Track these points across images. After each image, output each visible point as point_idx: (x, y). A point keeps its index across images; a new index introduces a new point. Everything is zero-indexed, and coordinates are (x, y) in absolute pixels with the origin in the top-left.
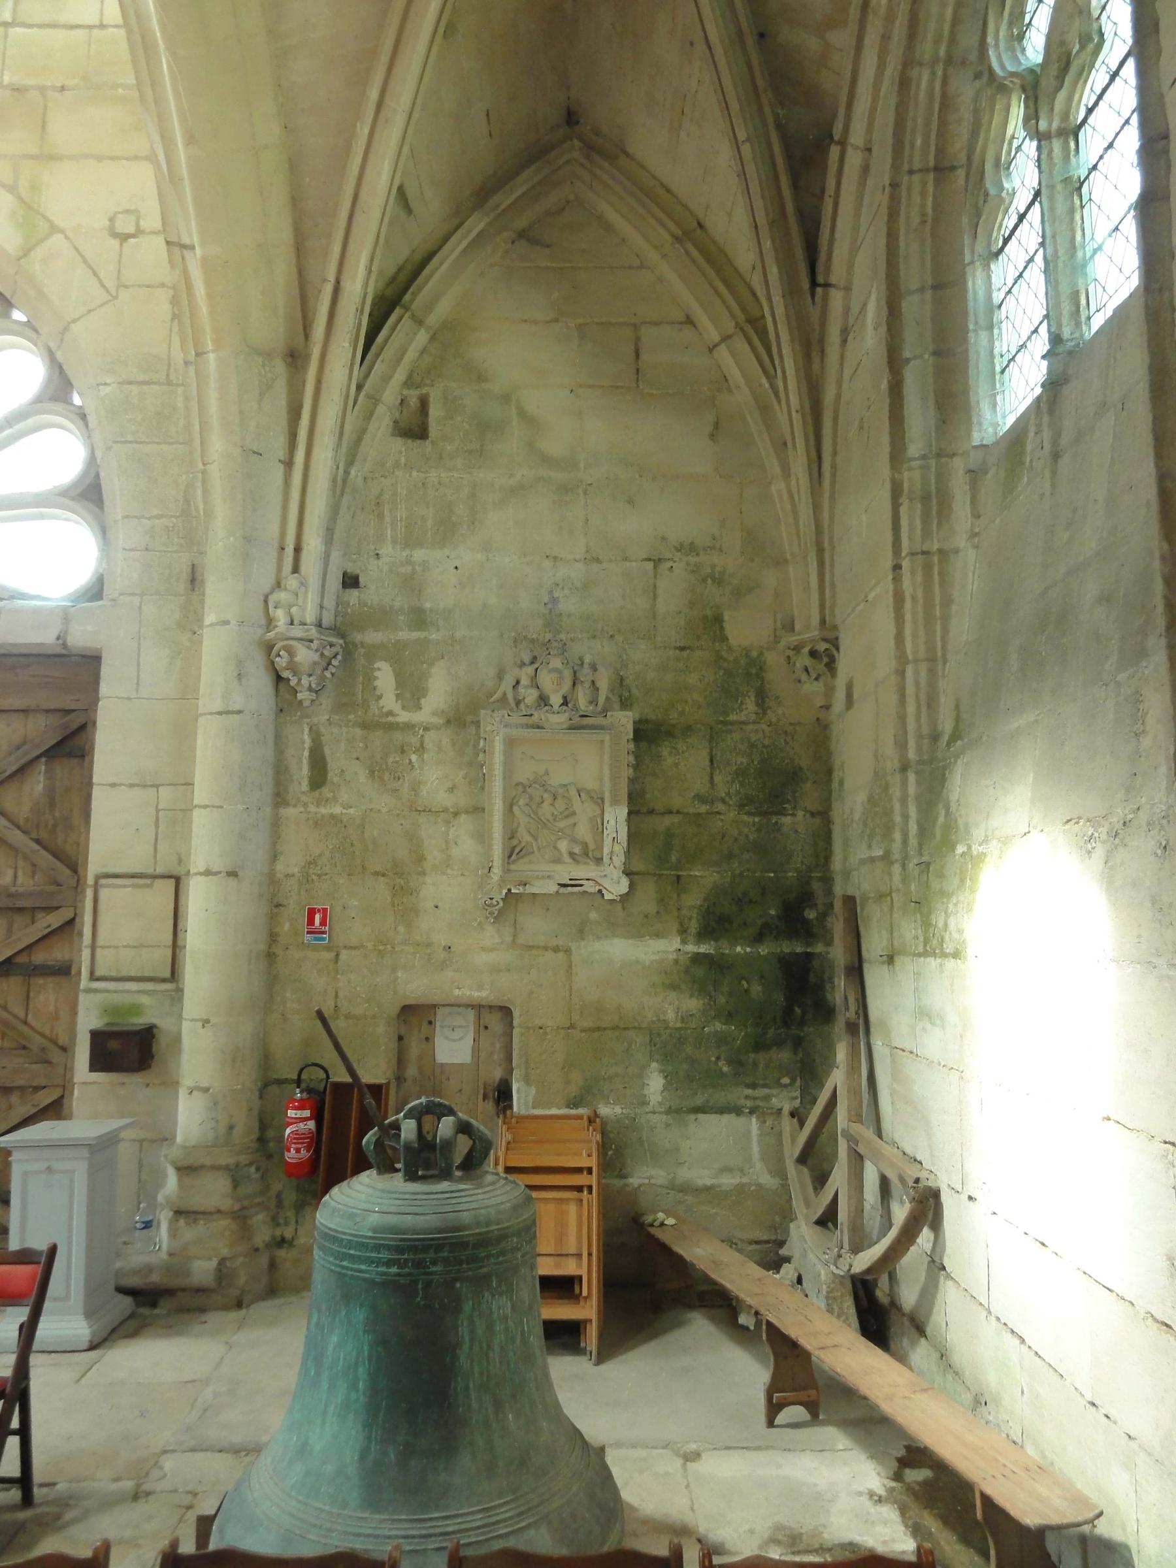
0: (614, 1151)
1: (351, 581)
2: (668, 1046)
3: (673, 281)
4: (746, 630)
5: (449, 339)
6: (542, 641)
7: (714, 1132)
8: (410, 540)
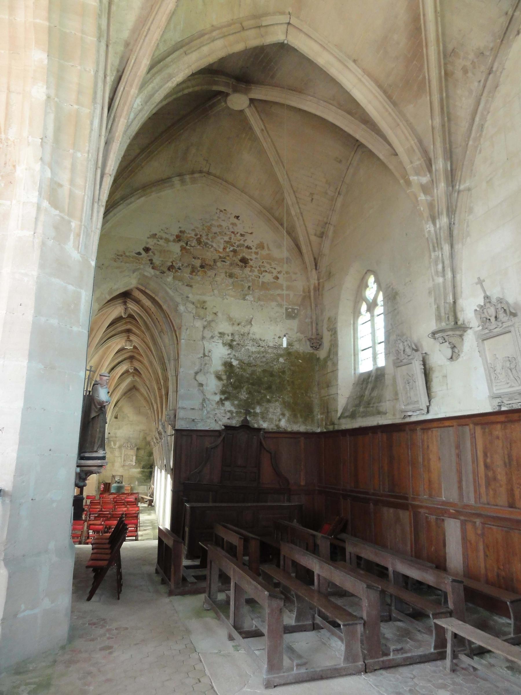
0: (132, 489)
1: (109, 433)
2: (138, 479)
3: (144, 403)
4: (149, 439)
5: (121, 409)
6: (128, 440)
7: (142, 487)
8: (116, 429)
